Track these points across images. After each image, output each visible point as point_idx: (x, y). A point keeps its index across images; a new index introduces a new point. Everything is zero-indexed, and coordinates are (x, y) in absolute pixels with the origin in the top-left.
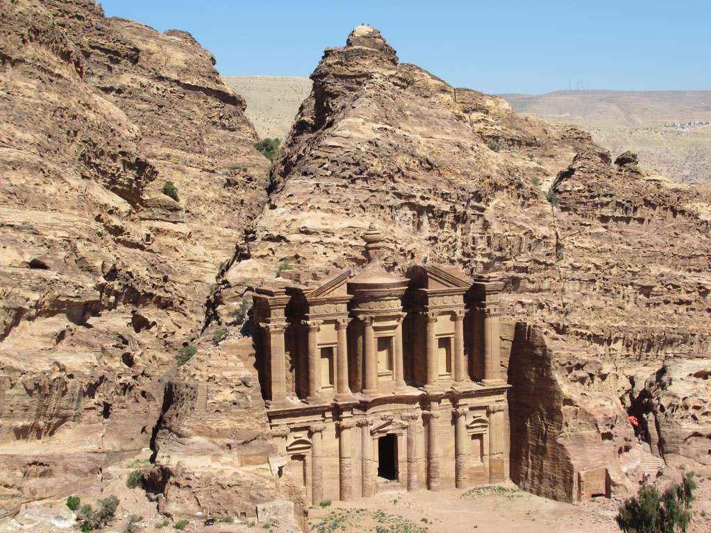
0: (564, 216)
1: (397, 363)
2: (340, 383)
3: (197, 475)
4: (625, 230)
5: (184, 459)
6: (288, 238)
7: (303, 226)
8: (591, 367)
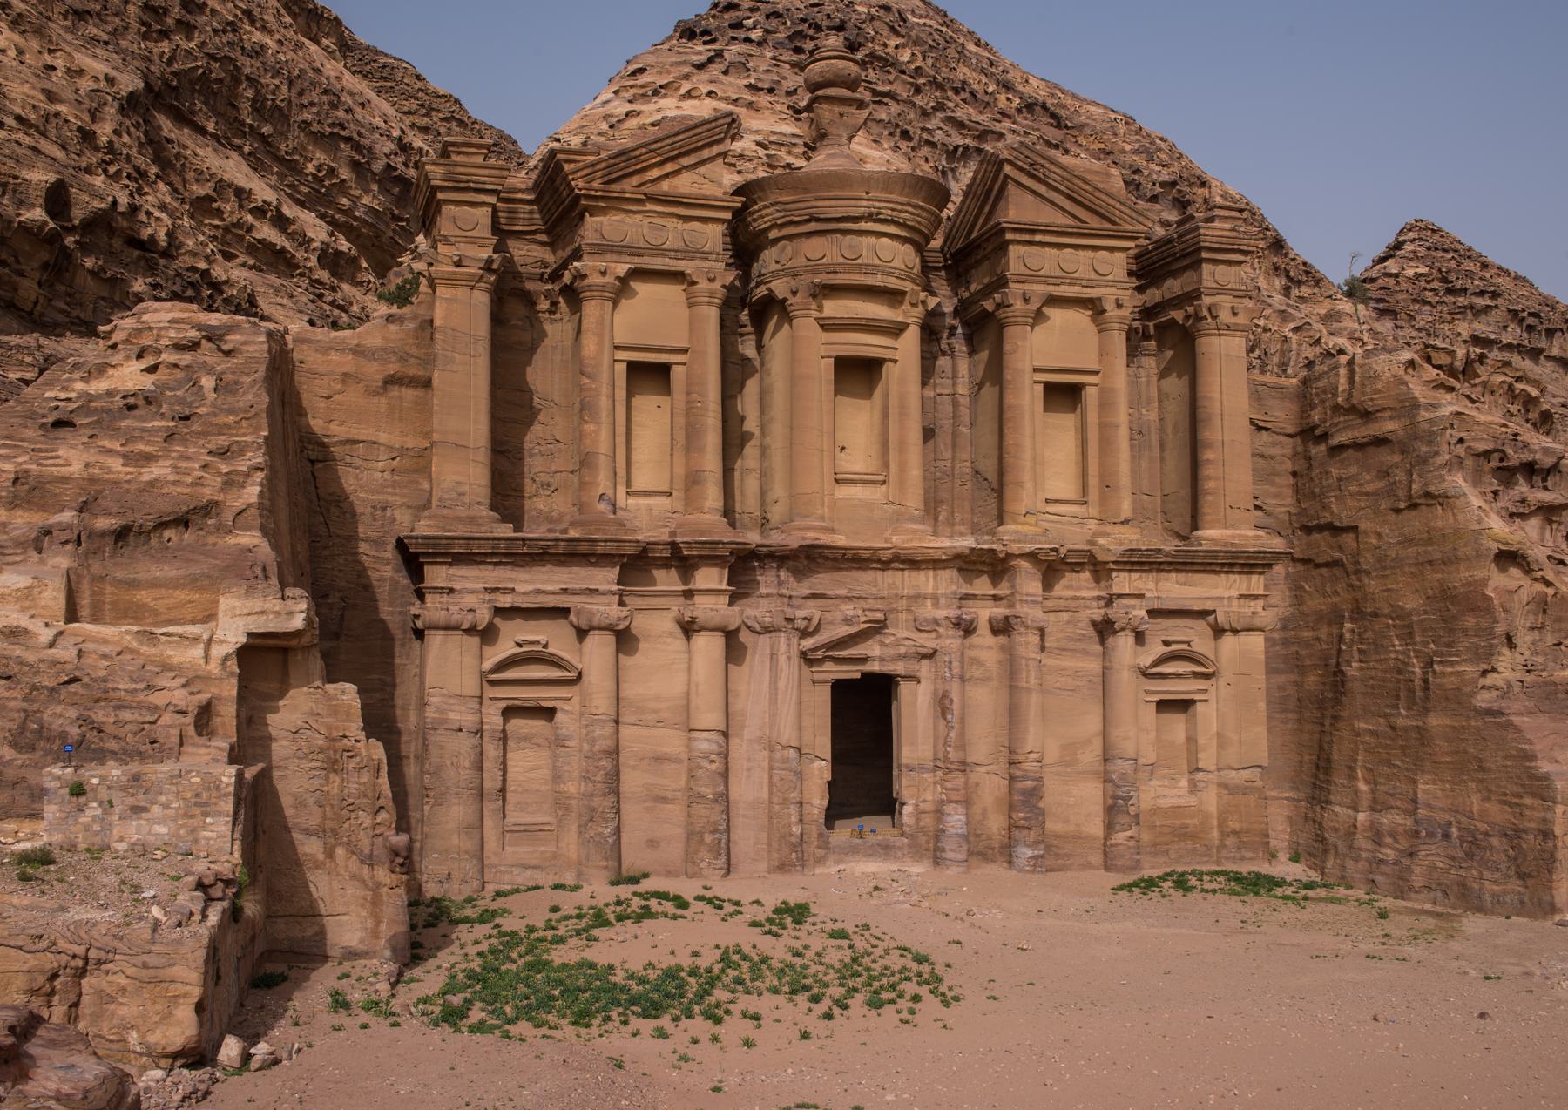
0: (1386, 326)
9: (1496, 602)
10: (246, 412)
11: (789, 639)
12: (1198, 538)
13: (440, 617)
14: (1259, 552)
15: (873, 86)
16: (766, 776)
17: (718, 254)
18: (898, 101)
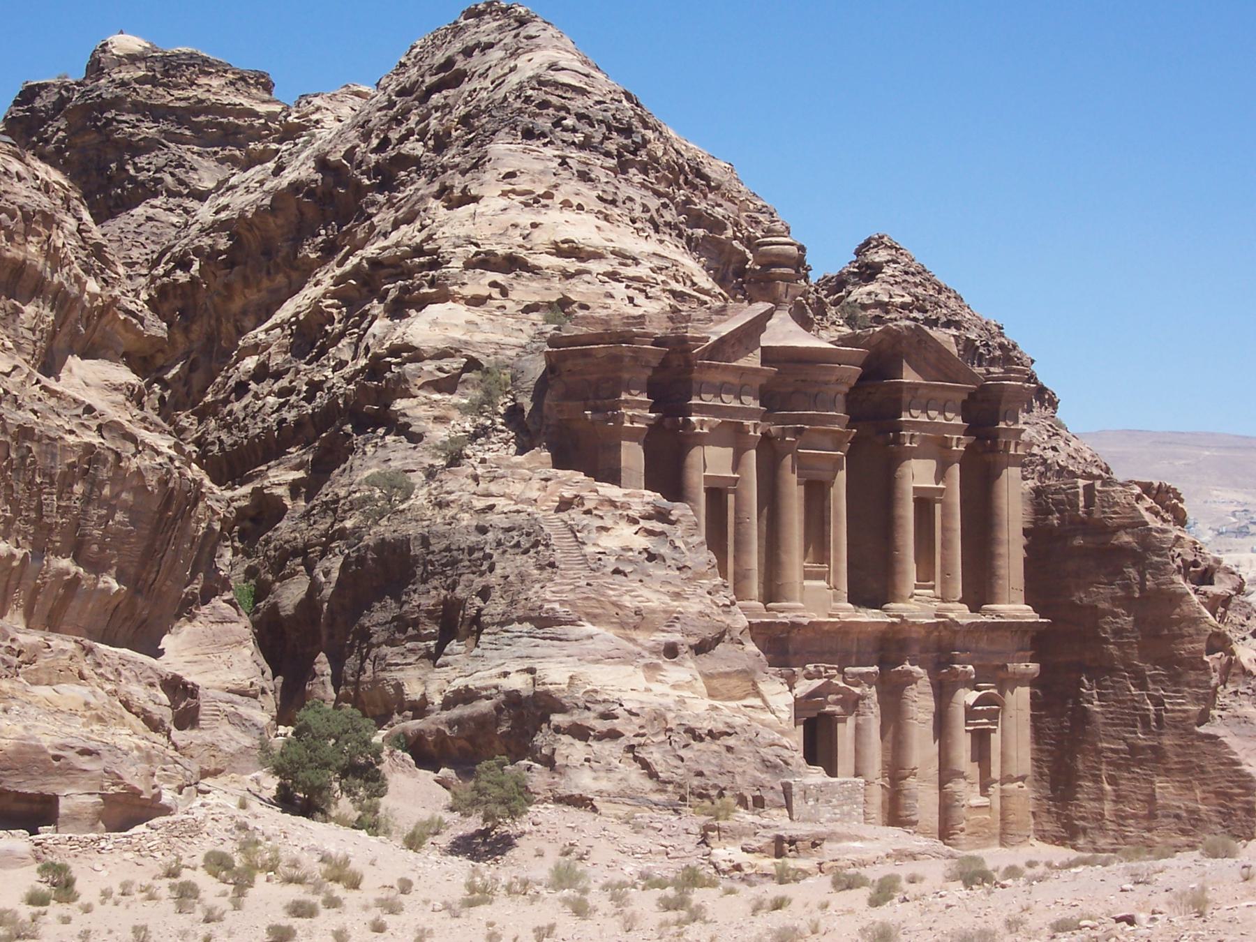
1: (837, 550)
3: (628, 706)
5: (582, 669)
6: (532, 260)
7: (563, 238)
9: (1211, 665)
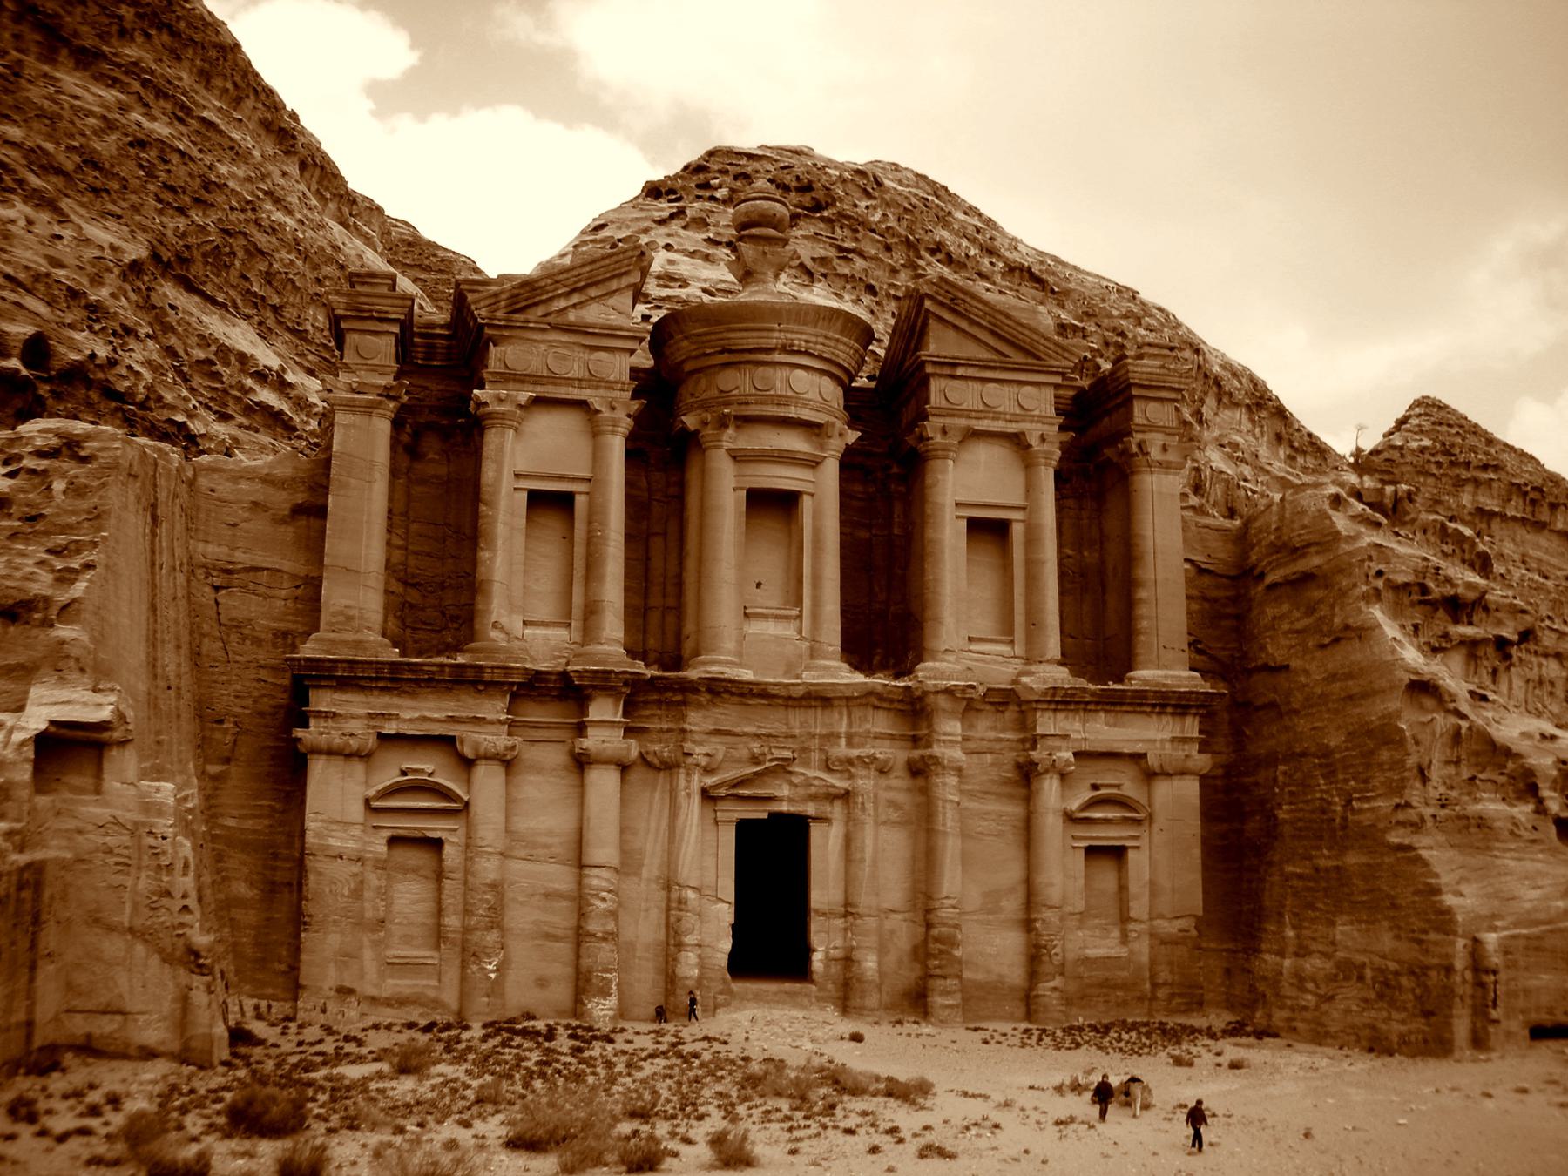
2: (592, 611)
4: (1531, 552)
8: (1499, 623)
9: (1407, 734)
10: (91, 513)
11: (688, 774)
12: (1131, 679)
13: (323, 741)
14: (1191, 693)
15: (839, 243)
16: (664, 916)
17: (623, 383)
18: (865, 258)
